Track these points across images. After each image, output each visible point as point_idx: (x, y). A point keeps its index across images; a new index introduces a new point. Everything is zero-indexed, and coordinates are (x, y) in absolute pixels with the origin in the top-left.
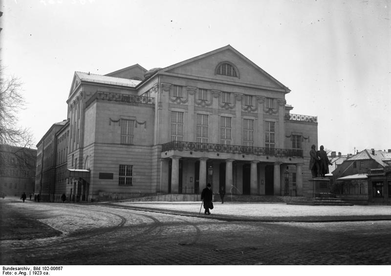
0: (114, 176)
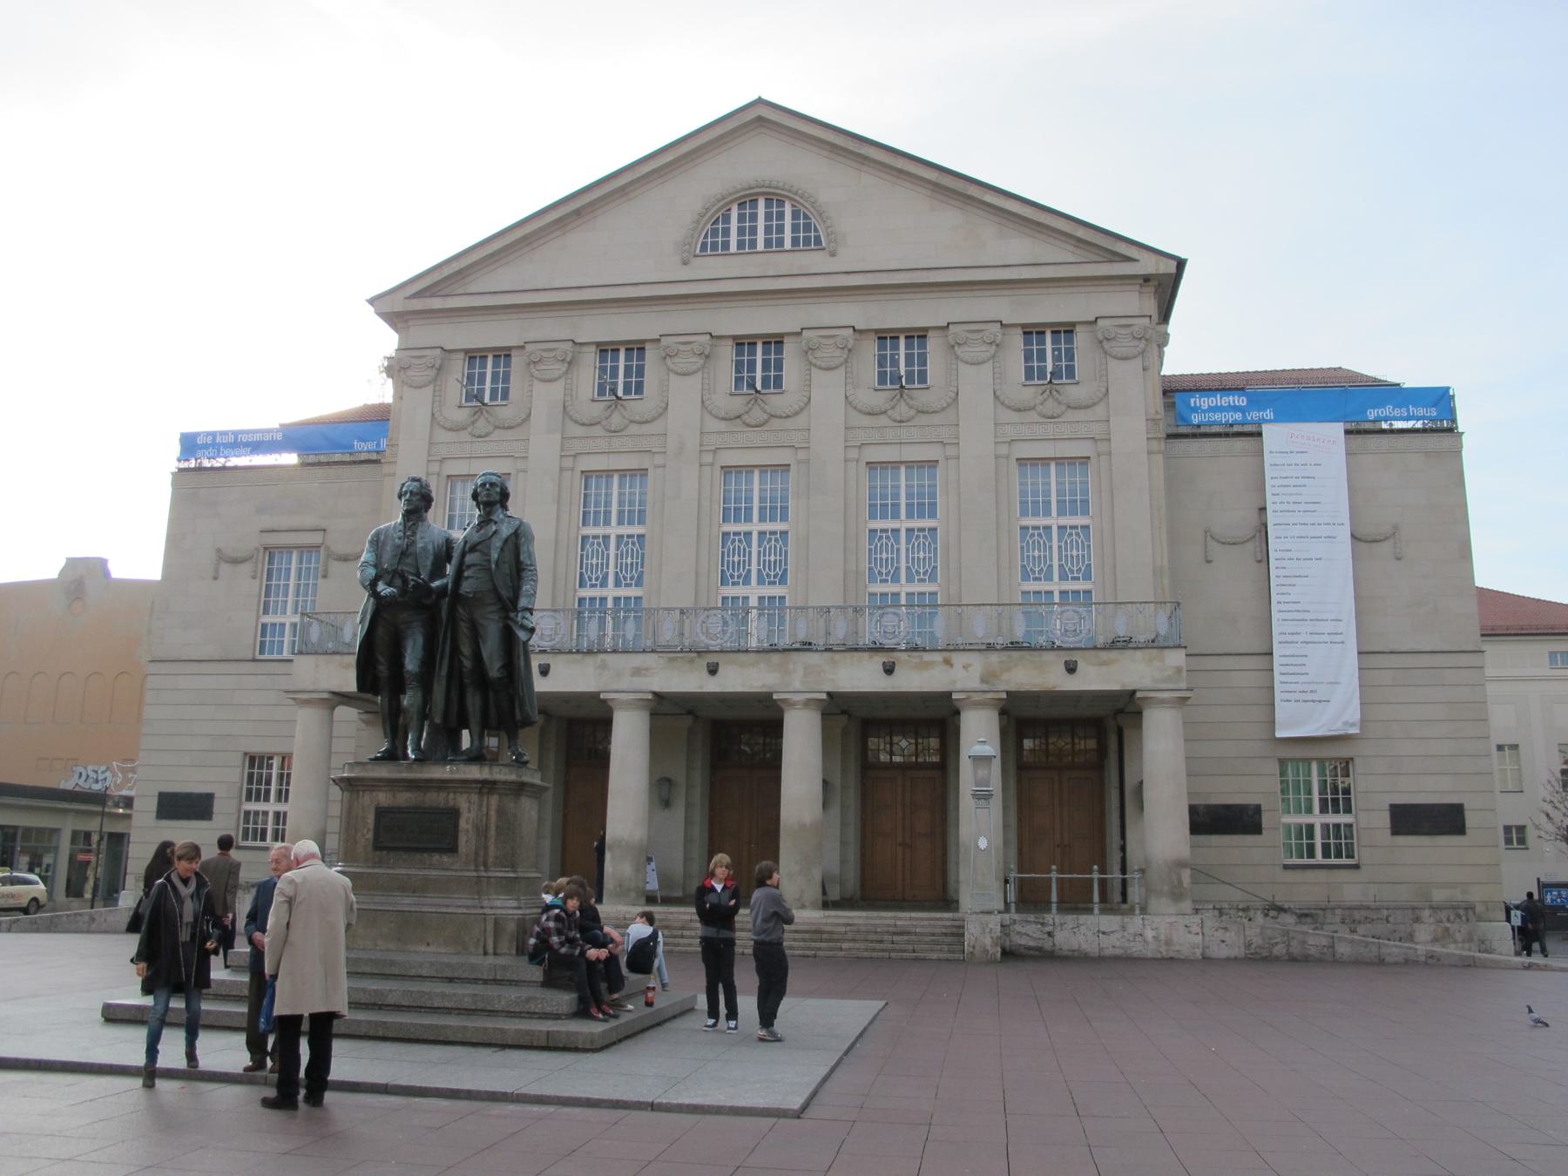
0: (218, 806)
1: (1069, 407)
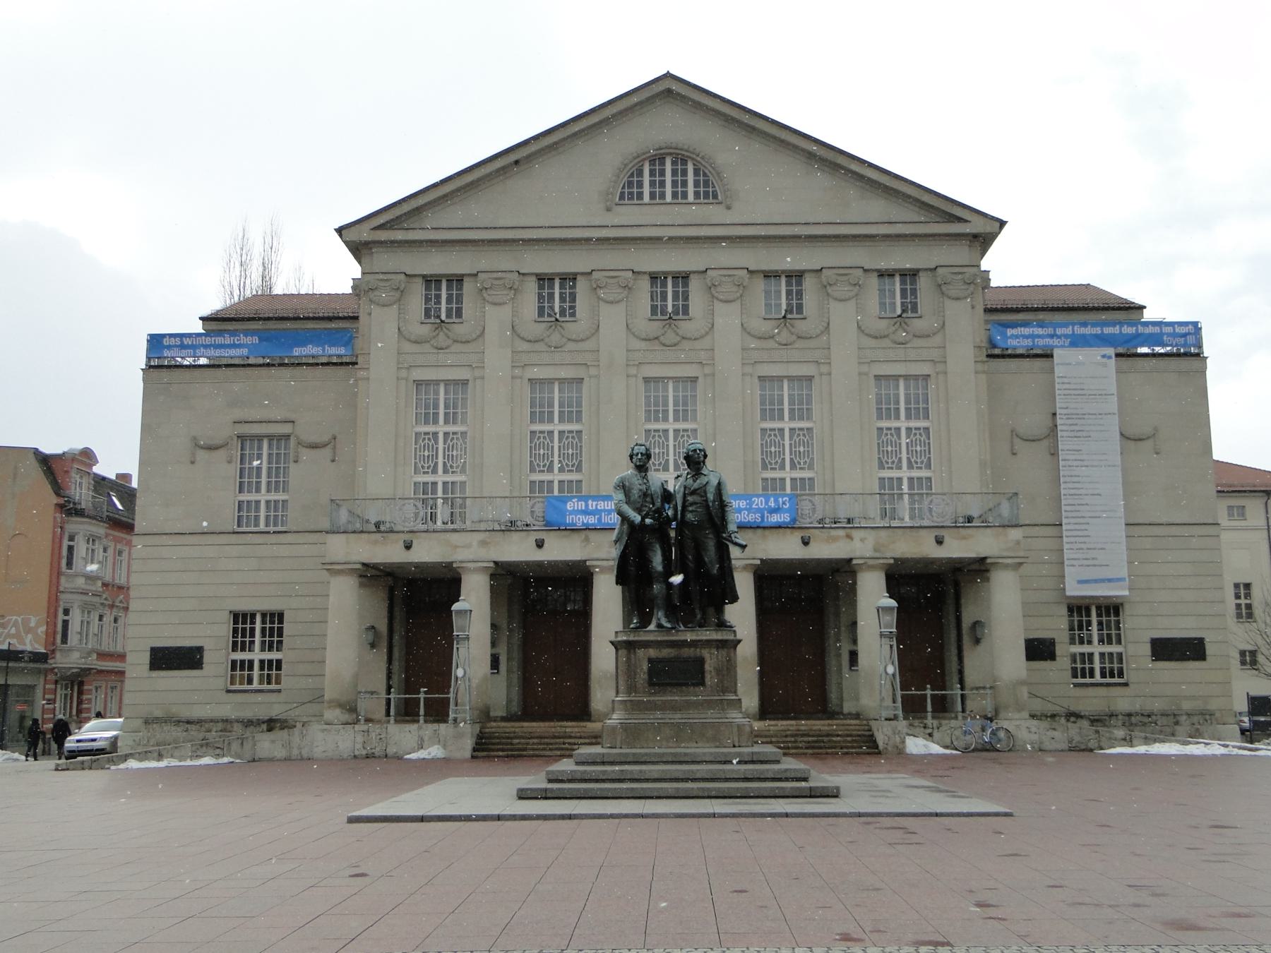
0: (207, 658)
1: (915, 336)
